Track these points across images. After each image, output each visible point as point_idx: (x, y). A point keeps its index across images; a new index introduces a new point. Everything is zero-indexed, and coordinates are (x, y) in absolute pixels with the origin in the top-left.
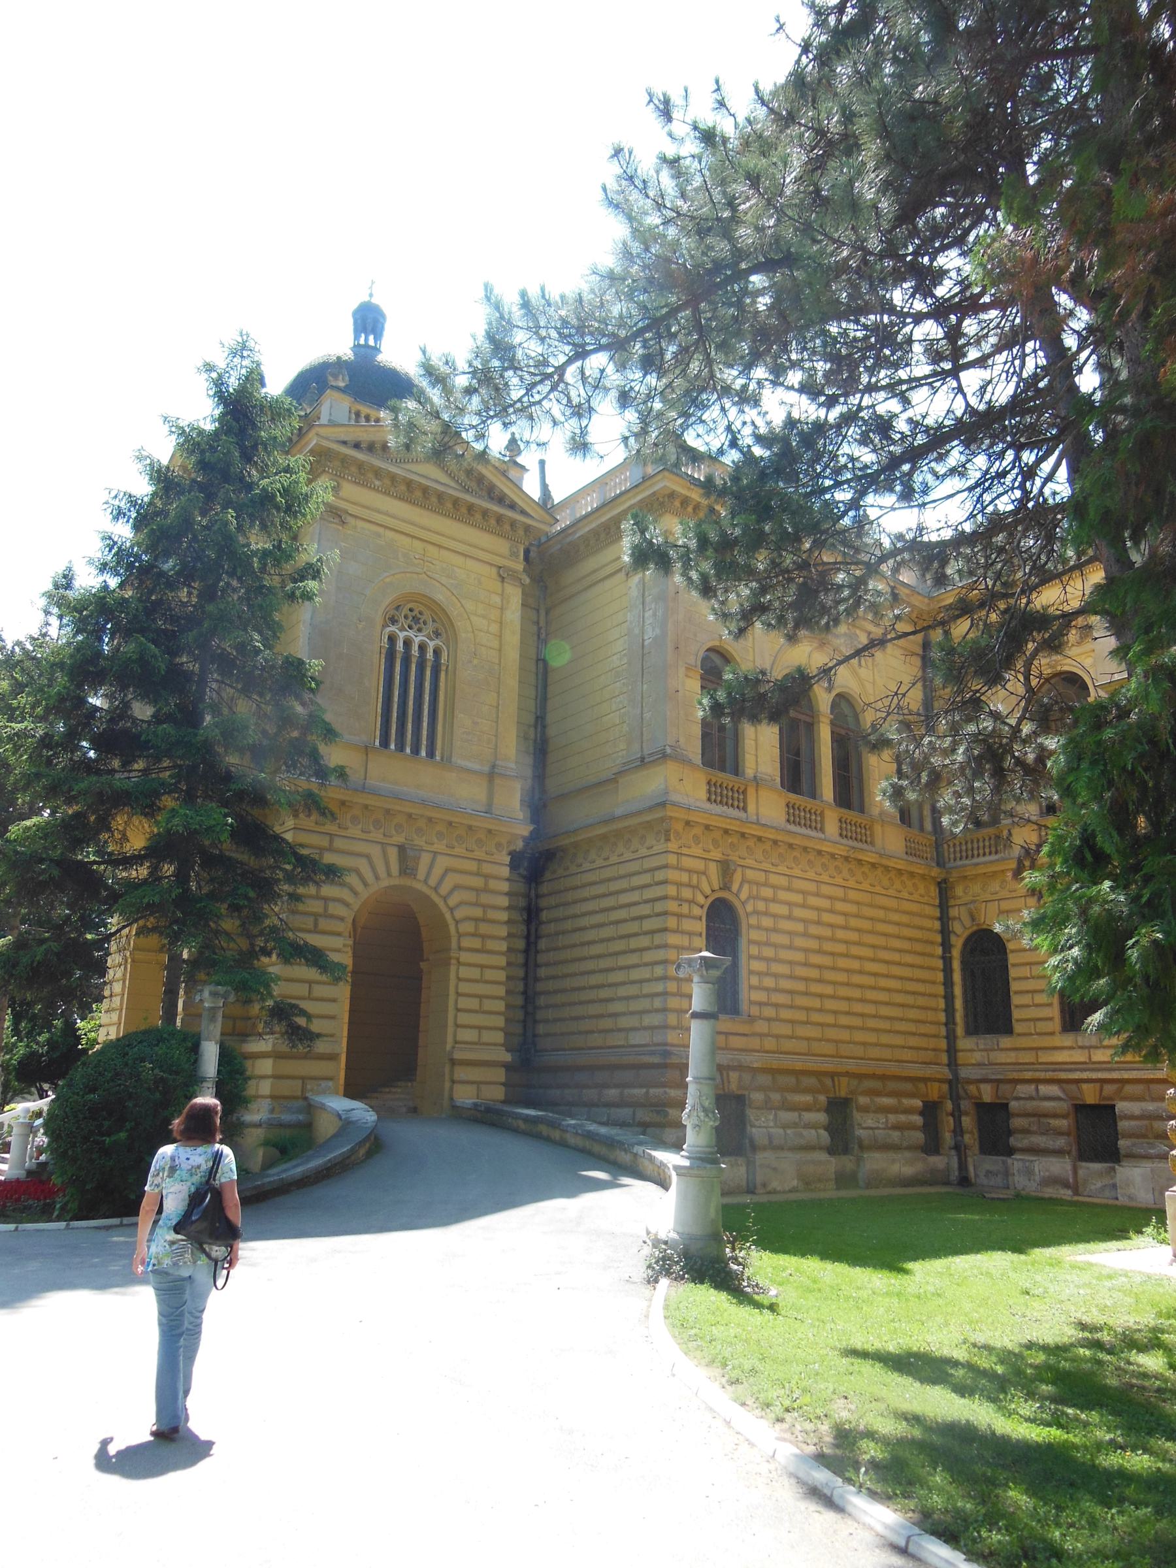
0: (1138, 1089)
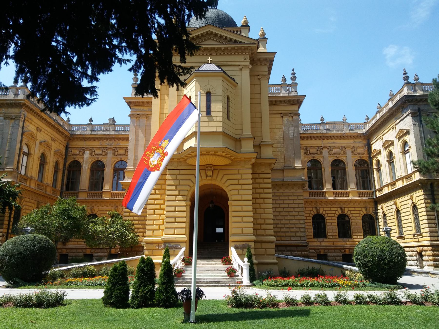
0: (333, 250)
